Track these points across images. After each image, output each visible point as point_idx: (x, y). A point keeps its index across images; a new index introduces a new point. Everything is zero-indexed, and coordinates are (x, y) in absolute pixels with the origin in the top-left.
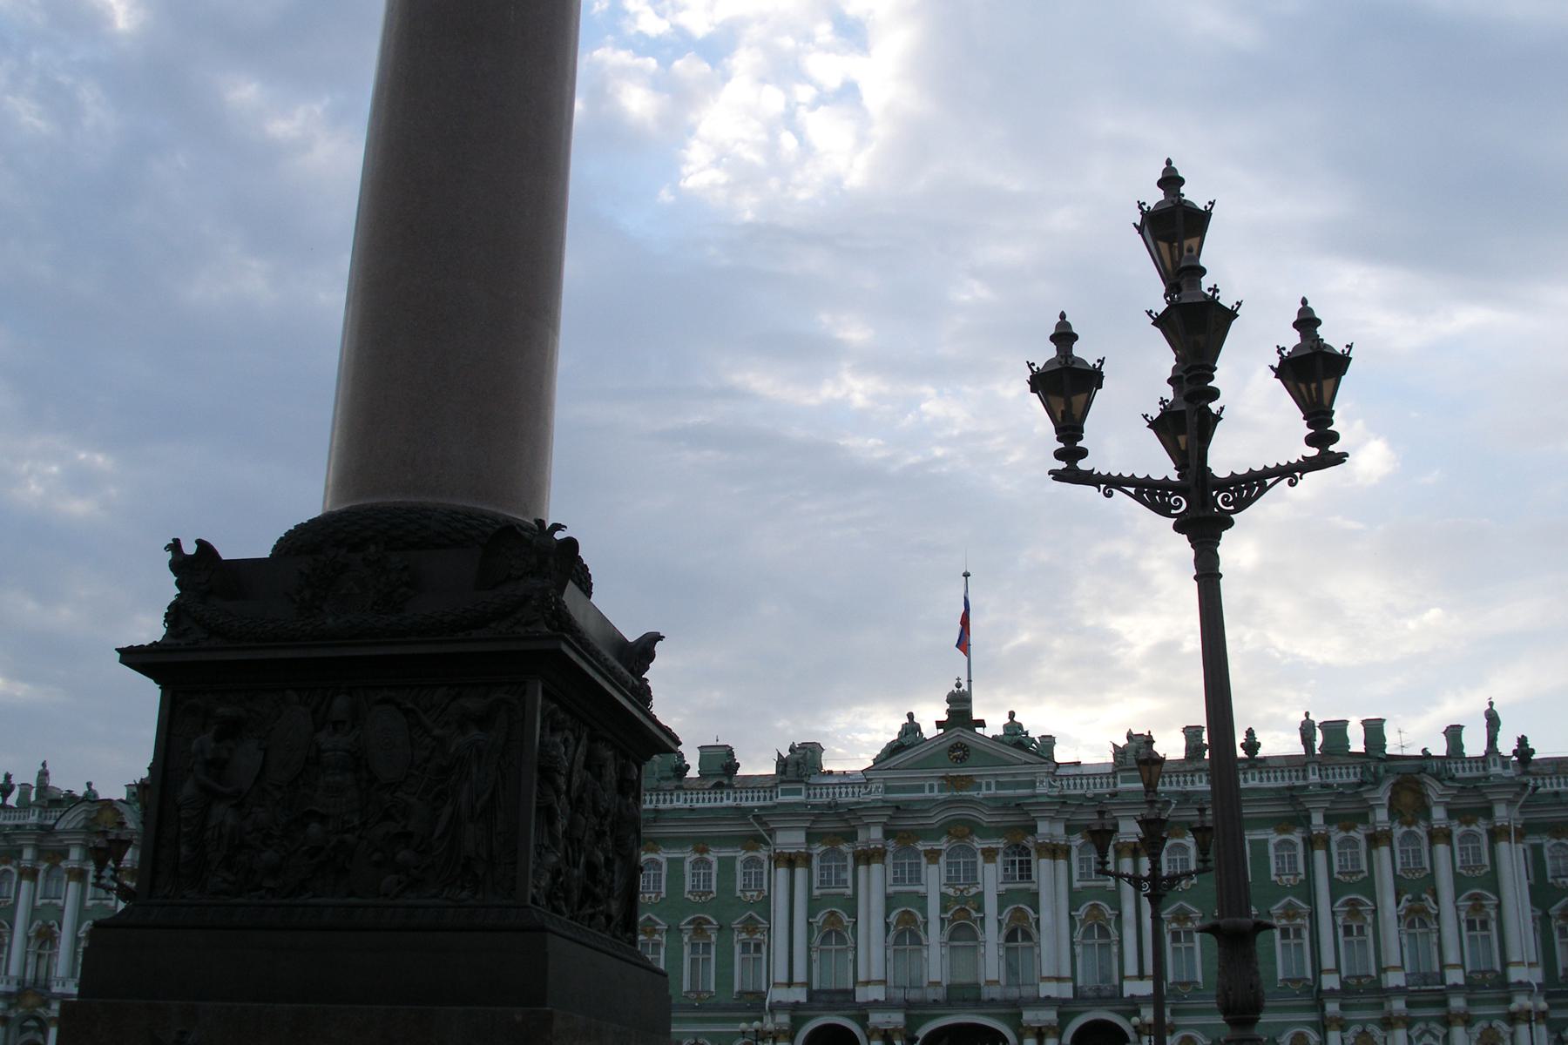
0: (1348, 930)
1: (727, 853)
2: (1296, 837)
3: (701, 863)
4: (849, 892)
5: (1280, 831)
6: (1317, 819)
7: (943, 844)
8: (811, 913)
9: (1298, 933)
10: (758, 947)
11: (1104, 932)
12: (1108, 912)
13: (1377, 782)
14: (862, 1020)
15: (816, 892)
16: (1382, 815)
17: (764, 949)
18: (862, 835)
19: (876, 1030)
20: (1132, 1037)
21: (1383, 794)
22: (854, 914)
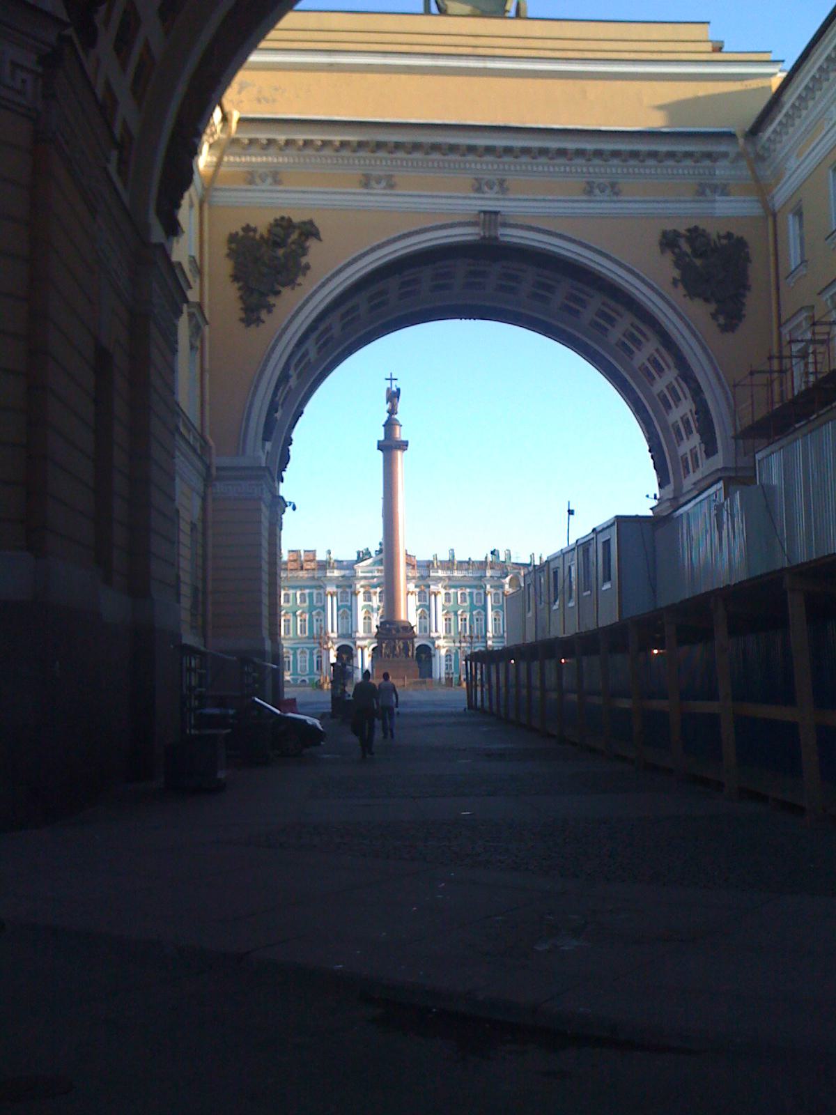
0: (495, 619)
1: (311, 591)
2: (482, 591)
3: (302, 595)
4: (349, 604)
5: (478, 589)
6: (488, 587)
7: (378, 590)
8: (338, 610)
9: (481, 620)
10: (321, 620)
11: (425, 618)
12: (427, 612)
13: (507, 576)
14: (355, 644)
15: (339, 604)
16: (507, 587)
17: (323, 621)
18: (353, 586)
19: (359, 647)
20: (433, 649)
21: (507, 580)
22: (351, 610)
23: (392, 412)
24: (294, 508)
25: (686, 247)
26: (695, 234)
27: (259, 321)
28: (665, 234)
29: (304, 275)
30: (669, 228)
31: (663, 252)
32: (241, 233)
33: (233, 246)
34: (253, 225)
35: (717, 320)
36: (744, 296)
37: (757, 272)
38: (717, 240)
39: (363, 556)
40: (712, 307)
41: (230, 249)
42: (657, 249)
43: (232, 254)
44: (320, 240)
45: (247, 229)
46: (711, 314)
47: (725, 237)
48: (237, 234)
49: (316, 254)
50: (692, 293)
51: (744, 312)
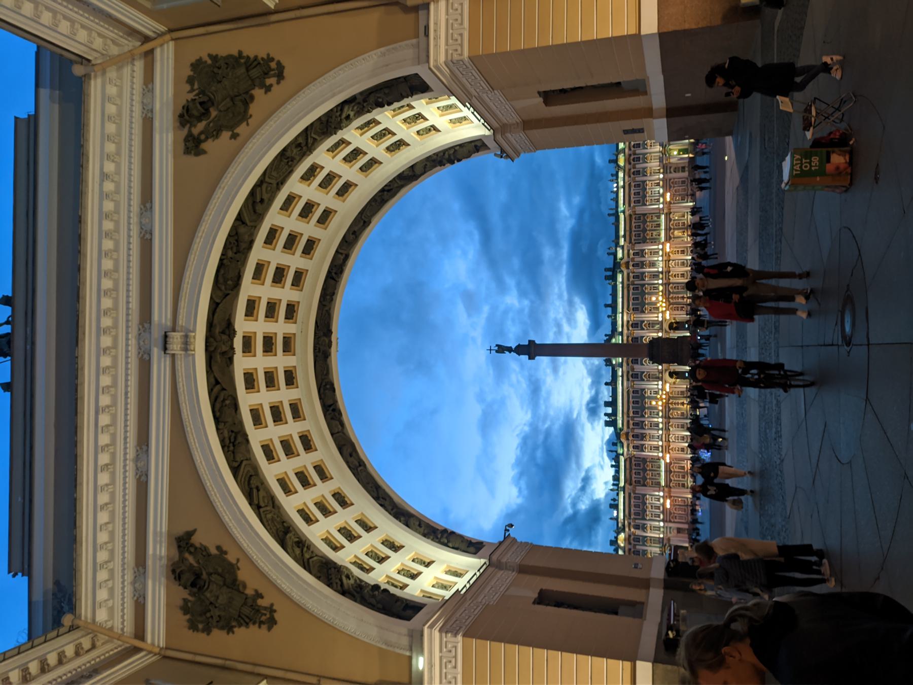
23: (510, 350)
24: (511, 526)
25: (201, 126)
26: (185, 116)
27: (271, 610)
28: (187, 151)
29: (226, 553)
30: (181, 147)
31: (204, 152)
32: (188, 617)
33: (200, 626)
34: (181, 603)
35: (271, 86)
36: (248, 57)
37: (226, 43)
38: (195, 93)
39: (608, 363)
40: (258, 93)
41: (203, 631)
42: (202, 157)
43: (208, 630)
44: (195, 531)
45: (185, 609)
46: (266, 93)
47: (192, 84)
48: (189, 621)
49: (205, 538)
50: (244, 116)
51: (265, 57)
